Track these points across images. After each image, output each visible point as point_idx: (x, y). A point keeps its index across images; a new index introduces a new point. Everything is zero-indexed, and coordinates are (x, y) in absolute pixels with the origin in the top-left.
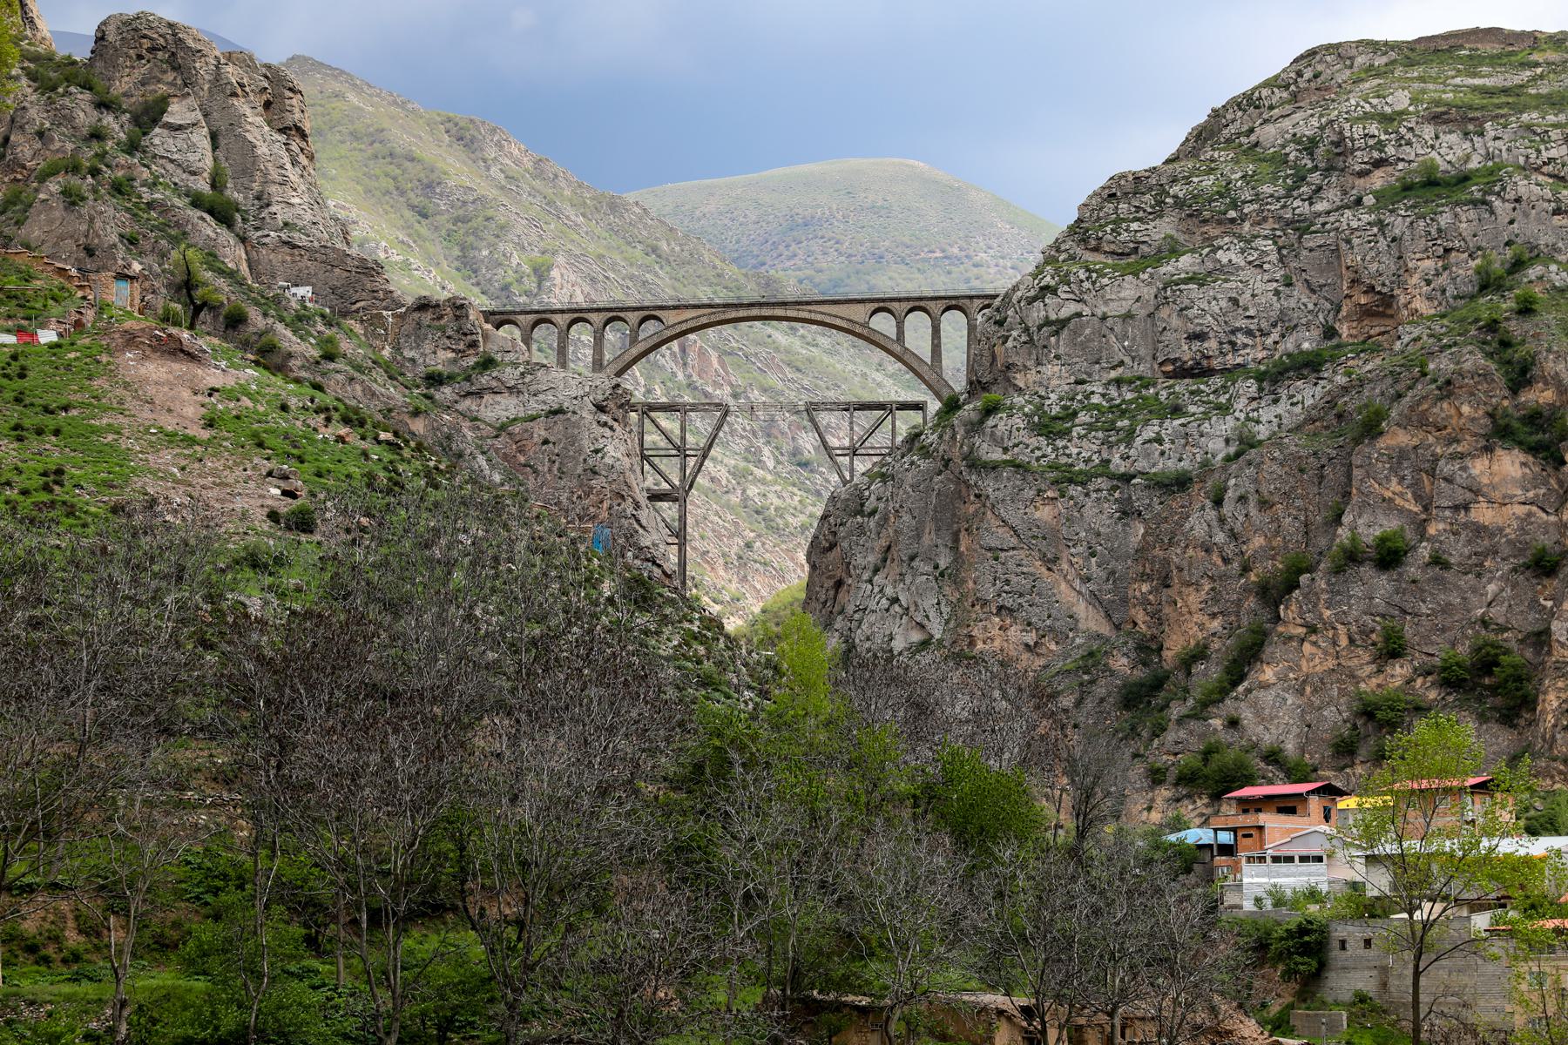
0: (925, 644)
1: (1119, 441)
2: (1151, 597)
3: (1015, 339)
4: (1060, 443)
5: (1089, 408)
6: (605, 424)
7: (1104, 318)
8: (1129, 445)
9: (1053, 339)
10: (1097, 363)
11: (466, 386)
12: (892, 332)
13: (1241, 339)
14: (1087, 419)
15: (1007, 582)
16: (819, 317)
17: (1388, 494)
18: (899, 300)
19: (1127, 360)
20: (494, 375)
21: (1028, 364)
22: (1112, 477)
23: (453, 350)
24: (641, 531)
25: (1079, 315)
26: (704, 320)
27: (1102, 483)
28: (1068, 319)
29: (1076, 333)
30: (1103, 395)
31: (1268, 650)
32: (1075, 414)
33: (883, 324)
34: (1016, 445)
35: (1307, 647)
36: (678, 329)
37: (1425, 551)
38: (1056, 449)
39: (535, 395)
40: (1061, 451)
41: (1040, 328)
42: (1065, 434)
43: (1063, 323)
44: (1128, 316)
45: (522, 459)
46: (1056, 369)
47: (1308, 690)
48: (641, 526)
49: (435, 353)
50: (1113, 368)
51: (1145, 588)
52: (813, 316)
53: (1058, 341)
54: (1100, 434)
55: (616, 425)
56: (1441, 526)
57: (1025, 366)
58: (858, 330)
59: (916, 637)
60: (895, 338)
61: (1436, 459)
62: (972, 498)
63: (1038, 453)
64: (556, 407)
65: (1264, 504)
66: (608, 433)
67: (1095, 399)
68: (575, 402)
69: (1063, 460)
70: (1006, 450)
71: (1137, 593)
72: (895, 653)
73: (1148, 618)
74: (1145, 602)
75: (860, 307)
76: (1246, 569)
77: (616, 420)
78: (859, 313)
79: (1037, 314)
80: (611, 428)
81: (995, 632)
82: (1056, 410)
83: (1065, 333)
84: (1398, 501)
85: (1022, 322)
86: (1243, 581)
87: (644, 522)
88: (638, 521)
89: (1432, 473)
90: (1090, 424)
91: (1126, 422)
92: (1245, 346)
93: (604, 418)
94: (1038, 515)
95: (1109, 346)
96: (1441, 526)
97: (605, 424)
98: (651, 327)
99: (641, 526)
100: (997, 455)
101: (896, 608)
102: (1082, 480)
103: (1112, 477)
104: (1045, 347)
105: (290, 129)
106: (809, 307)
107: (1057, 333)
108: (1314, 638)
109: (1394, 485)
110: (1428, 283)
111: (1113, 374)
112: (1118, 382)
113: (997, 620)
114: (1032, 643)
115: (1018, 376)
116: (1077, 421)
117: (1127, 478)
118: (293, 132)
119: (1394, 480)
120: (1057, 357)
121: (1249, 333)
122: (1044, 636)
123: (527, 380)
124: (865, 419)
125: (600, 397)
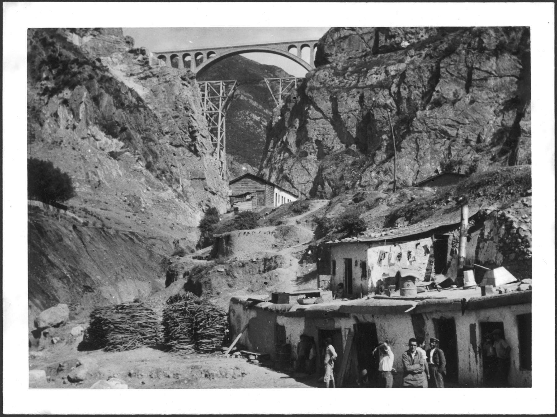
6: (184, 85)
18: (299, 42)
24: (193, 121)
48: (194, 119)
55: (189, 85)
66: (185, 87)
75: (284, 45)
78: (284, 48)
79: (336, 36)
80: (186, 86)
87: (195, 118)
88: (193, 117)
93: (184, 82)
99: (194, 119)
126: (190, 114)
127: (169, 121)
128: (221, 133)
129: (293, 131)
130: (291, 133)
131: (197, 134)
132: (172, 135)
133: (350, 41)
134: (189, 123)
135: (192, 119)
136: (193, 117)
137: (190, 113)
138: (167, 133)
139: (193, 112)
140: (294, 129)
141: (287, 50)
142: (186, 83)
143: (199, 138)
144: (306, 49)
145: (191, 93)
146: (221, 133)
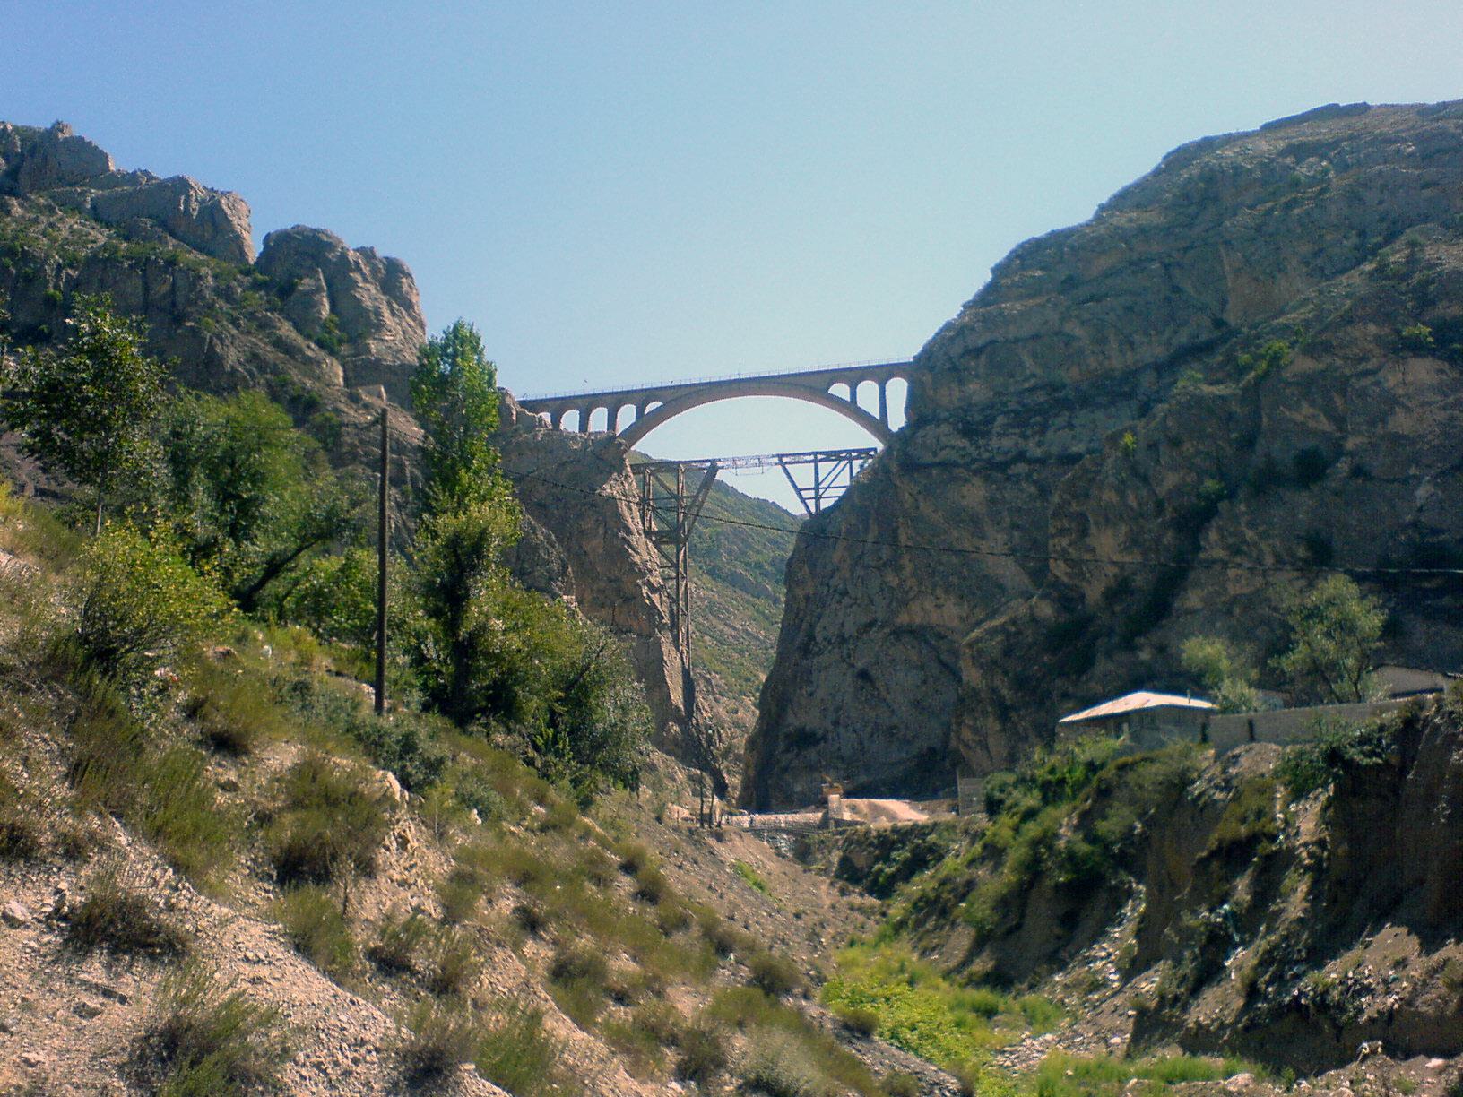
0: (871, 625)
1: (1036, 433)
2: (1070, 550)
4: (981, 442)
5: (1006, 413)
7: (1017, 340)
8: (1043, 432)
10: (1012, 376)
12: (848, 398)
13: (1137, 338)
14: (1006, 421)
15: (940, 563)
17: (1299, 418)
19: (1039, 371)
22: (1030, 462)
25: (993, 342)
27: (1021, 468)
30: (1019, 403)
31: (1192, 575)
32: (994, 419)
33: (840, 390)
34: (942, 449)
35: (1231, 573)
37: (1343, 466)
38: (978, 447)
40: (983, 449)
41: (962, 356)
42: (986, 434)
44: (1036, 337)
46: (977, 387)
47: (1237, 610)
50: (1026, 380)
51: (1065, 542)
54: (1017, 431)
56: (1358, 440)
59: (864, 619)
61: (1348, 378)
62: (907, 496)
63: (962, 453)
65: (1175, 443)
67: (1012, 406)
69: (986, 455)
70: (935, 454)
71: (1059, 548)
72: (846, 636)
73: (1068, 570)
74: (1064, 555)
76: (1160, 507)
81: (928, 605)
82: (978, 417)
83: (983, 358)
84: (1311, 424)
86: (1160, 520)
88: (630, 545)
89: (1343, 393)
90: (1007, 424)
91: (1038, 419)
92: (1142, 343)
94: (965, 502)
95: (1021, 364)
96: (1358, 440)
98: (653, 406)
100: (928, 458)
101: (846, 601)
102: (1003, 466)
103: (1030, 462)
104: (967, 369)
106: (779, 380)
107: (977, 357)
108: (1238, 560)
109: (1306, 409)
110: (1307, 264)
111: (1027, 385)
112: (1031, 390)
113: (932, 597)
114: (965, 615)
117: (1042, 462)
119: (1305, 404)
120: (977, 376)
121: (1146, 333)
122: (975, 607)
124: (825, 467)
126: (622, 534)
139: (629, 532)
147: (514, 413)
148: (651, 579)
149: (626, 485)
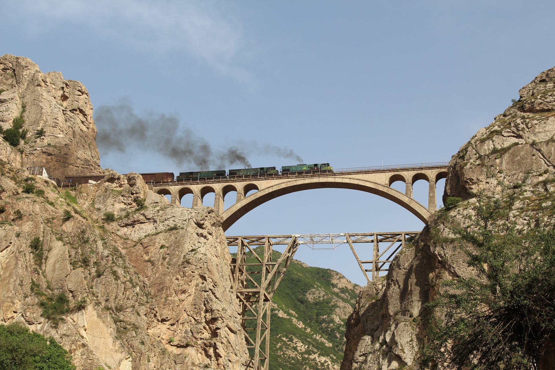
3: (471, 164)
6: (202, 235)
9: (498, 161)
11: (125, 221)
16: (356, 182)
20: (142, 213)
21: (480, 178)
23: (125, 204)
25: (517, 144)
26: (284, 186)
28: (509, 148)
29: (513, 155)
36: (267, 192)
39: (163, 222)
43: (504, 151)
45: (147, 258)
48: (216, 298)
49: (113, 205)
52: (352, 182)
53: (501, 163)
57: (478, 179)
58: (381, 188)
60: (404, 193)
64: (172, 226)
66: (202, 240)
68: (184, 222)
75: (382, 175)
77: (210, 234)
78: (382, 179)
79: (488, 146)
80: (205, 237)
83: (506, 156)
85: (477, 152)
88: (213, 294)
90: (522, 209)
93: (200, 231)
97: (202, 235)
105: (76, 110)
115: (473, 187)
116: (513, 207)
118: (78, 112)
123: (160, 214)
125: (200, 218)
127: (170, 298)
128: (263, 332)
129: (406, 321)
130: (401, 325)
131: (219, 324)
132: (172, 325)
133: (513, 155)
134: (206, 302)
135: (212, 296)
136: (213, 294)
137: (209, 285)
138: (163, 321)
140: (407, 317)
141: (387, 182)
142: (205, 232)
143: (223, 332)
144: (420, 183)
145: (213, 251)
146: (263, 332)
147: (142, 192)
148: (229, 323)
149: (219, 248)
